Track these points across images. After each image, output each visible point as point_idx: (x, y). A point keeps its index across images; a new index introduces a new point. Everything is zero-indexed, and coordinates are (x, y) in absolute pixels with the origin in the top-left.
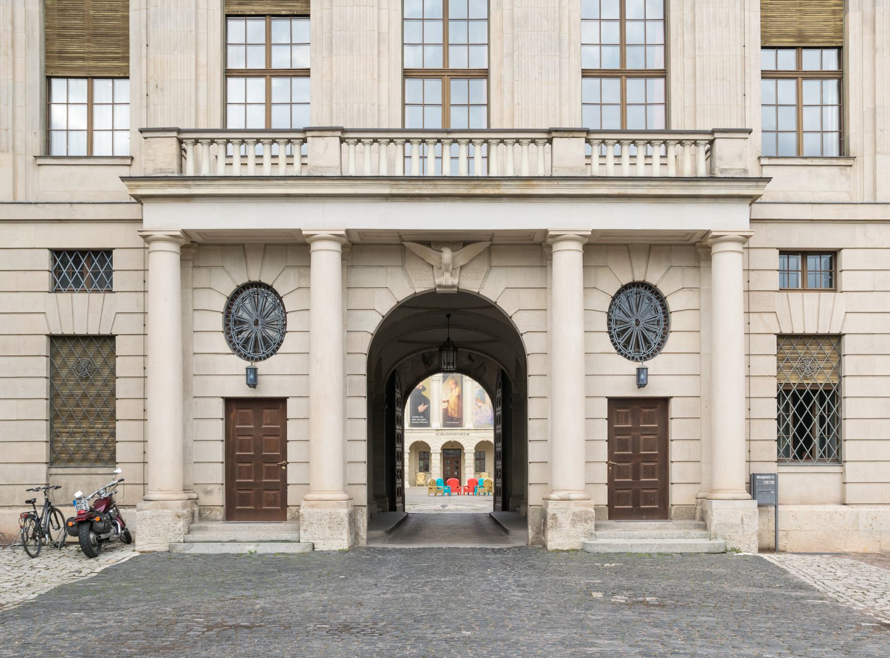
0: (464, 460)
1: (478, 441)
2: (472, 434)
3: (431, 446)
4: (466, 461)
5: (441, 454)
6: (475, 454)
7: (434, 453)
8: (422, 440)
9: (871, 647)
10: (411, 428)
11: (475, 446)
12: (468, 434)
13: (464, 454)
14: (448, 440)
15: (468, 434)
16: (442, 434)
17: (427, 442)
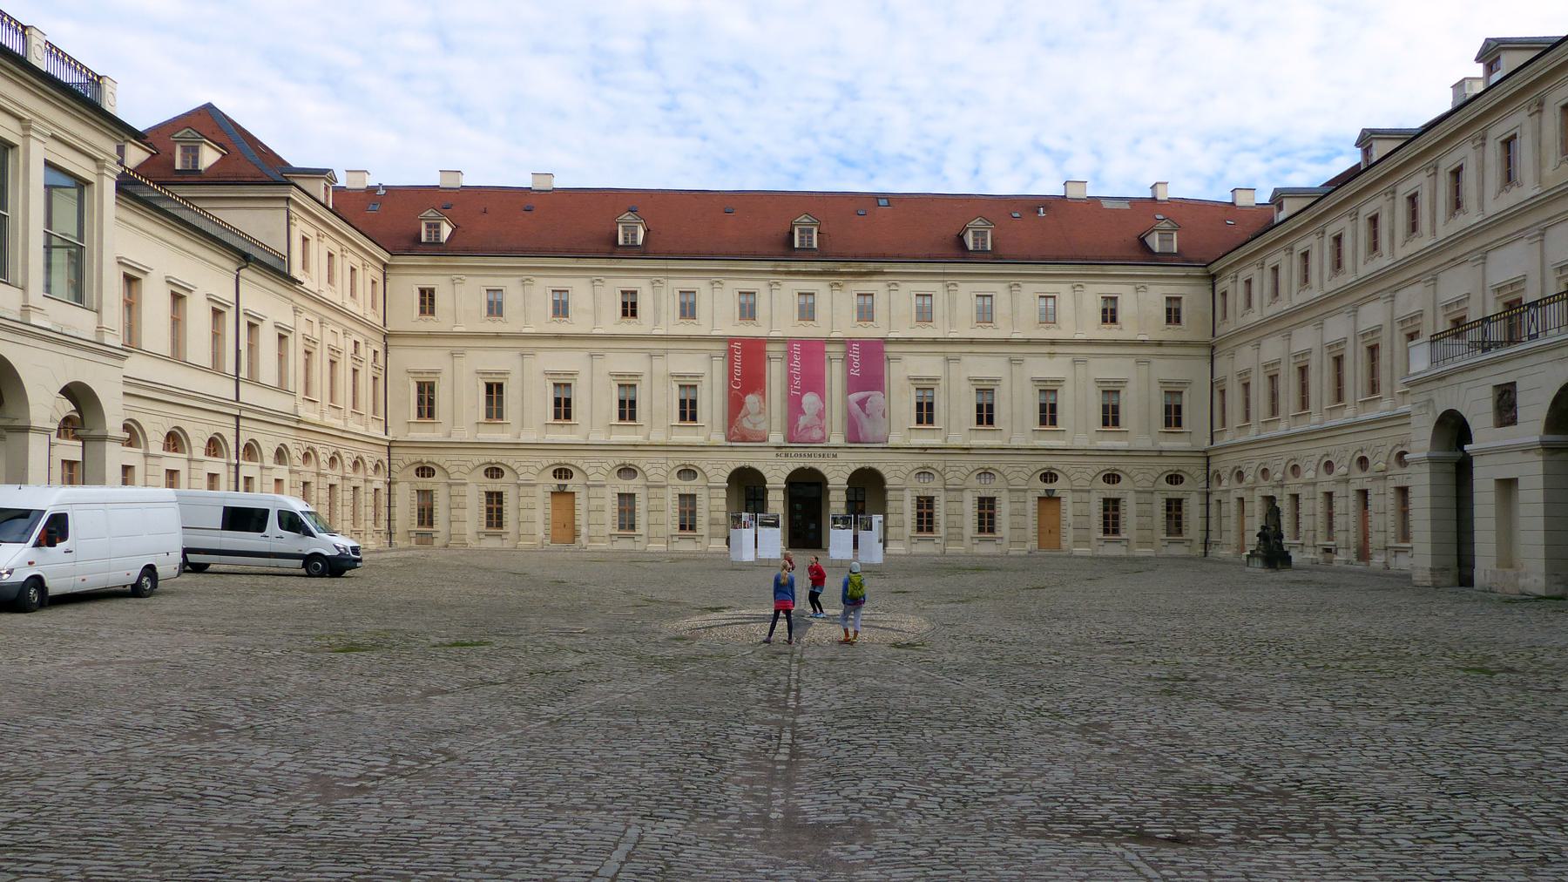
0: (828, 503)
1: (854, 469)
2: (842, 456)
3: (767, 476)
4: (832, 505)
5: (785, 490)
6: (847, 492)
7: (772, 489)
8: (752, 465)
9: (1497, 876)
10: (729, 444)
11: (847, 477)
12: (835, 456)
13: (828, 492)
14: (797, 466)
15: (835, 456)
16: (786, 455)
17: (760, 469)
